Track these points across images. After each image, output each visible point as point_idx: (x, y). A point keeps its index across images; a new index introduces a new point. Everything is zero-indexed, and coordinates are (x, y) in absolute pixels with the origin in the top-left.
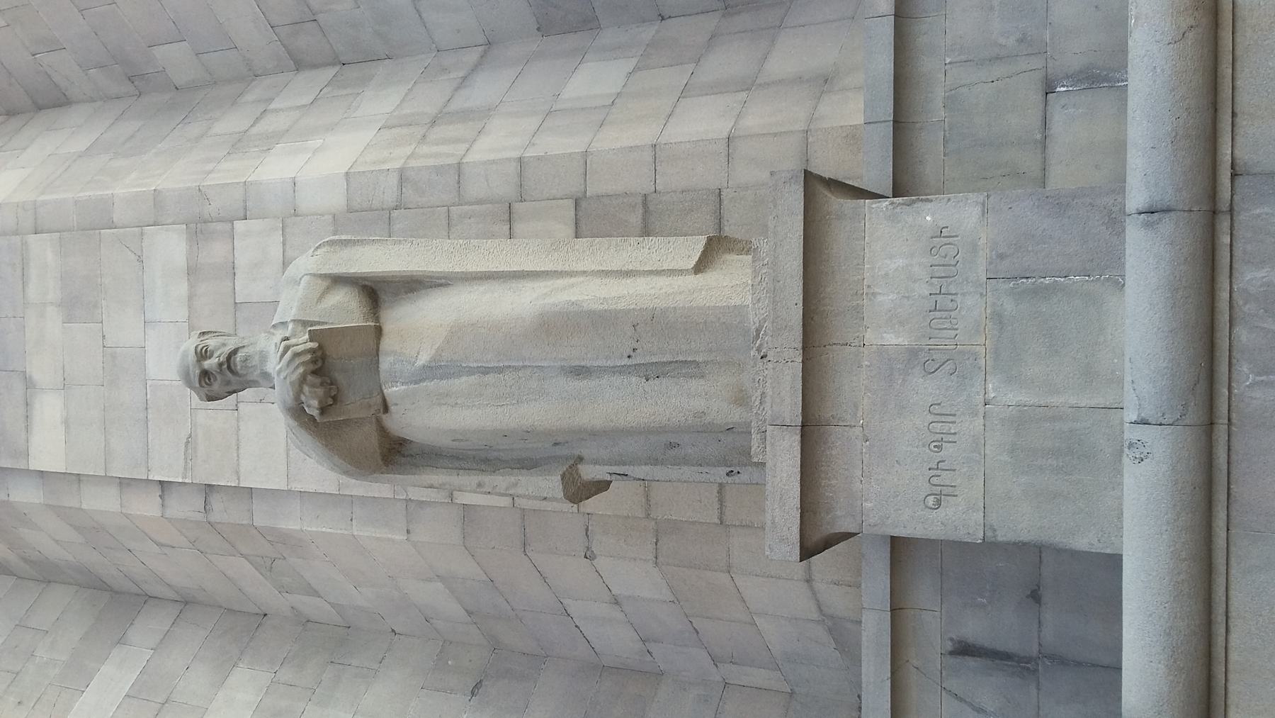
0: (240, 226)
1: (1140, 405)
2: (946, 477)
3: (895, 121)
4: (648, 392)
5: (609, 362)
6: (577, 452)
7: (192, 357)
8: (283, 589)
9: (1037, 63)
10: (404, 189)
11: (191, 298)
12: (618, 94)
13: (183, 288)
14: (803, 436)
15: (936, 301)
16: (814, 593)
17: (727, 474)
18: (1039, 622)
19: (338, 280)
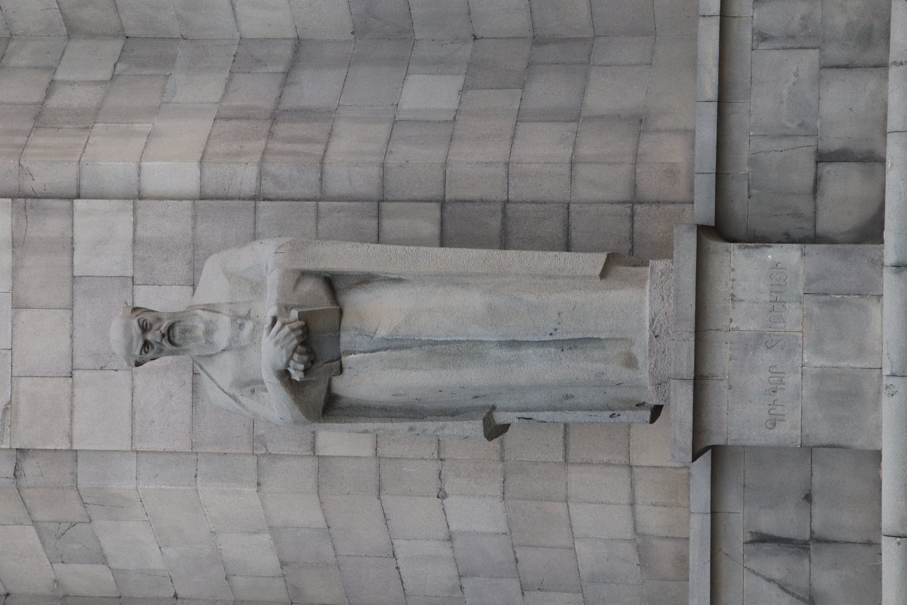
1: (892, 366)
2: (779, 410)
3: (717, 174)
4: (562, 359)
5: (536, 338)
6: (491, 403)
9: (812, 142)
10: (263, 182)
11: (15, 270)
12: (457, 111)
14: (695, 385)
15: (774, 306)
16: (634, 514)
17: (611, 416)
18: (811, 516)
19: (305, 274)
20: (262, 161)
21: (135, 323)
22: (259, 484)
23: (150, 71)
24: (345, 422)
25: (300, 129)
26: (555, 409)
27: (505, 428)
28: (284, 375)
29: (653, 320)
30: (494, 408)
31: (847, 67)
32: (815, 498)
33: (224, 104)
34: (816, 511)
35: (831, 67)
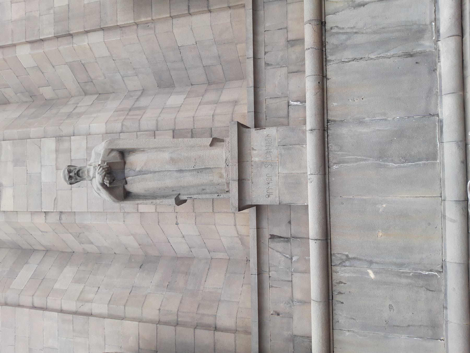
0: (72, 138)
2: (270, 191)
7: (66, 172)
8: (81, 243)
10: (123, 128)
11: (57, 158)
13: (54, 156)
16: (236, 229)
17: (218, 196)
19: (112, 150)
20: (123, 121)
21: (66, 170)
22: (124, 221)
23: (102, 101)
24: (132, 201)
25: (137, 112)
26: (199, 194)
27: (185, 201)
28: (103, 185)
29: (226, 159)
30: (179, 194)
31: (296, 72)
32: (292, 223)
33: (118, 108)
34: (292, 227)
35: (292, 73)
